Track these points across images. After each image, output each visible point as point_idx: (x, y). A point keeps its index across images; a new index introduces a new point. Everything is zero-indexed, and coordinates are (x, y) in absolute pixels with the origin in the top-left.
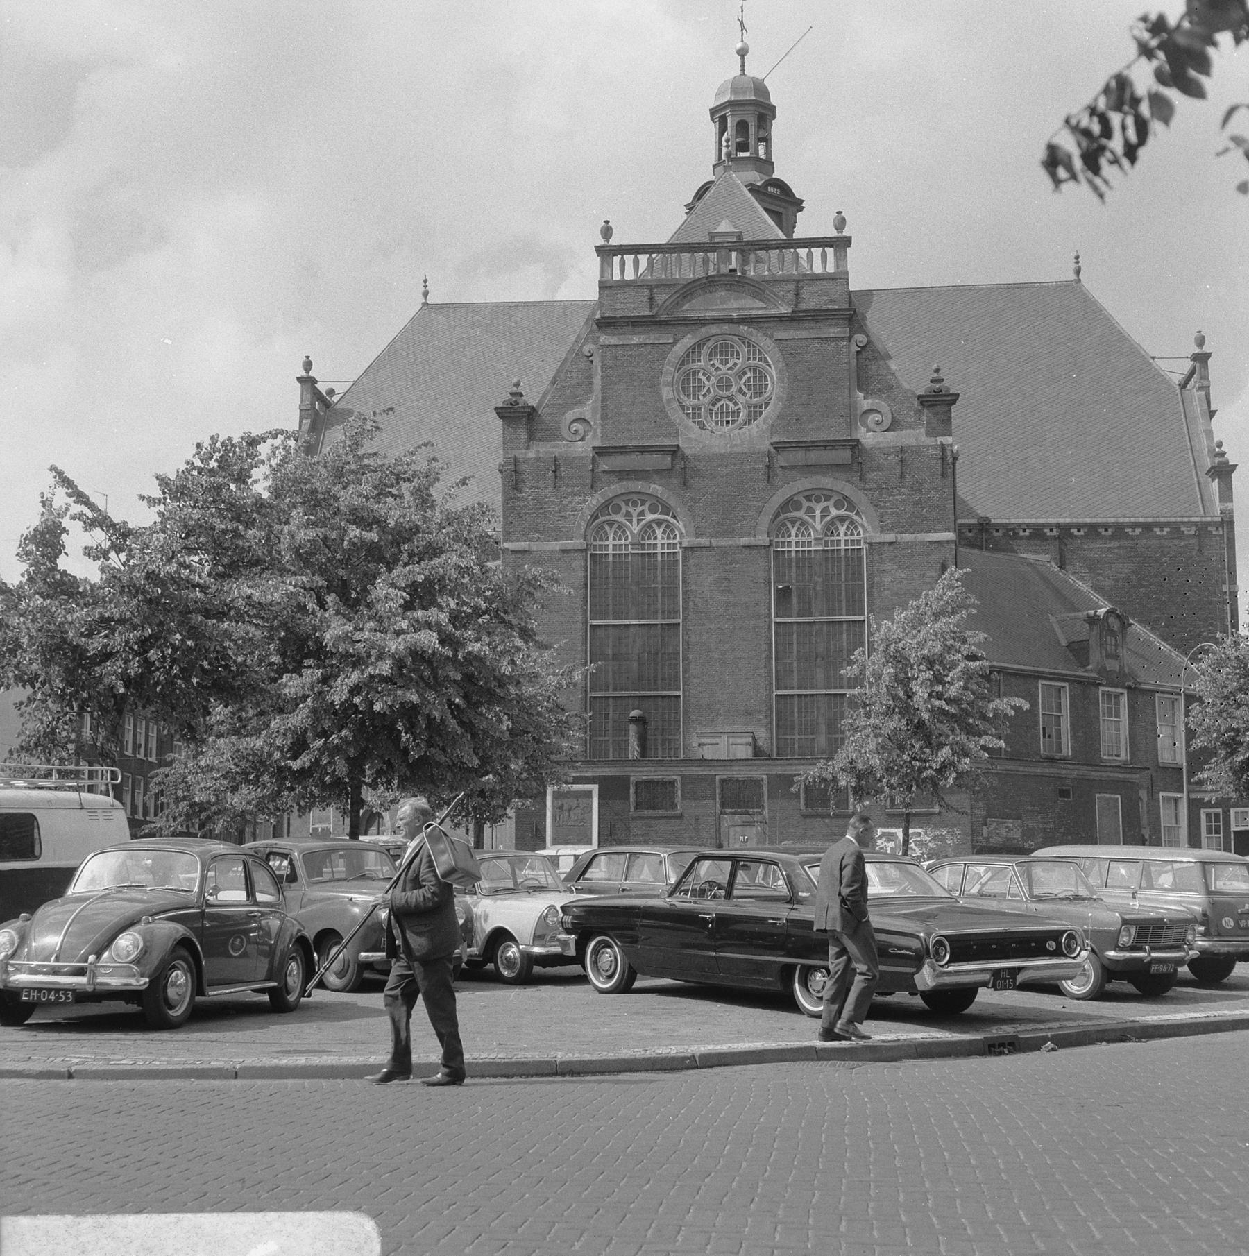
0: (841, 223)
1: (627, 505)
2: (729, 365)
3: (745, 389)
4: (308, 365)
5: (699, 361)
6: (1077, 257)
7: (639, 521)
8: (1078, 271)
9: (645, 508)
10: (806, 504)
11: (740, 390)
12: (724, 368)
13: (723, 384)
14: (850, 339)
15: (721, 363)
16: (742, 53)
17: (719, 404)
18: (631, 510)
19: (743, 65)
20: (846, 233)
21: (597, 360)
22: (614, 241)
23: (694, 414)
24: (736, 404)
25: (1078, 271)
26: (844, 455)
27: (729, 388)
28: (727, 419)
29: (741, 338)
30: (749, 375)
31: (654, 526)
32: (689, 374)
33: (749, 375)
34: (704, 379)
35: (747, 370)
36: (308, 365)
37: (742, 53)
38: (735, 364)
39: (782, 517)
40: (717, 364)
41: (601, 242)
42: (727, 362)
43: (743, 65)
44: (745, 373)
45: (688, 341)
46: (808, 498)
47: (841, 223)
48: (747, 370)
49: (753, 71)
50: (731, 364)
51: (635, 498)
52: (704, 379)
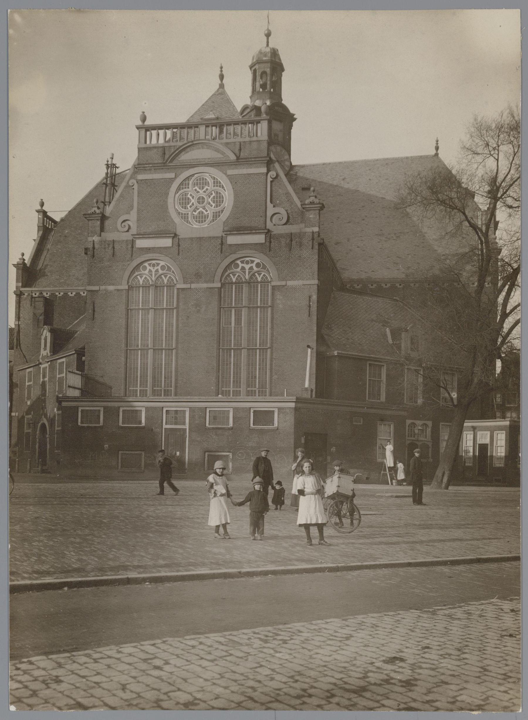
2: (204, 190)
3: (212, 203)
4: (42, 204)
5: (188, 188)
6: (437, 141)
7: (155, 275)
8: (437, 148)
10: (241, 265)
11: (209, 203)
12: (201, 192)
13: (201, 200)
14: (267, 174)
15: (200, 189)
17: (198, 211)
21: (136, 187)
22: (148, 123)
23: (185, 217)
24: (207, 211)
25: (437, 148)
26: (260, 238)
27: (203, 202)
28: (201, 218)
30: (214, 194)
31: (163, 276)
32: (183, 196)
34: (191, 198)
35: (213, 192)
36: (42, 204)
38: (207, 189)
39: (229, 272)
40: (198, 190)
41: (140, 123)
42: (203, 188)
44: (212, 194)
46: (242, 262)
48: (213, 192)
50: (205, 189)
51: (154, 262)
52: (191, 198)
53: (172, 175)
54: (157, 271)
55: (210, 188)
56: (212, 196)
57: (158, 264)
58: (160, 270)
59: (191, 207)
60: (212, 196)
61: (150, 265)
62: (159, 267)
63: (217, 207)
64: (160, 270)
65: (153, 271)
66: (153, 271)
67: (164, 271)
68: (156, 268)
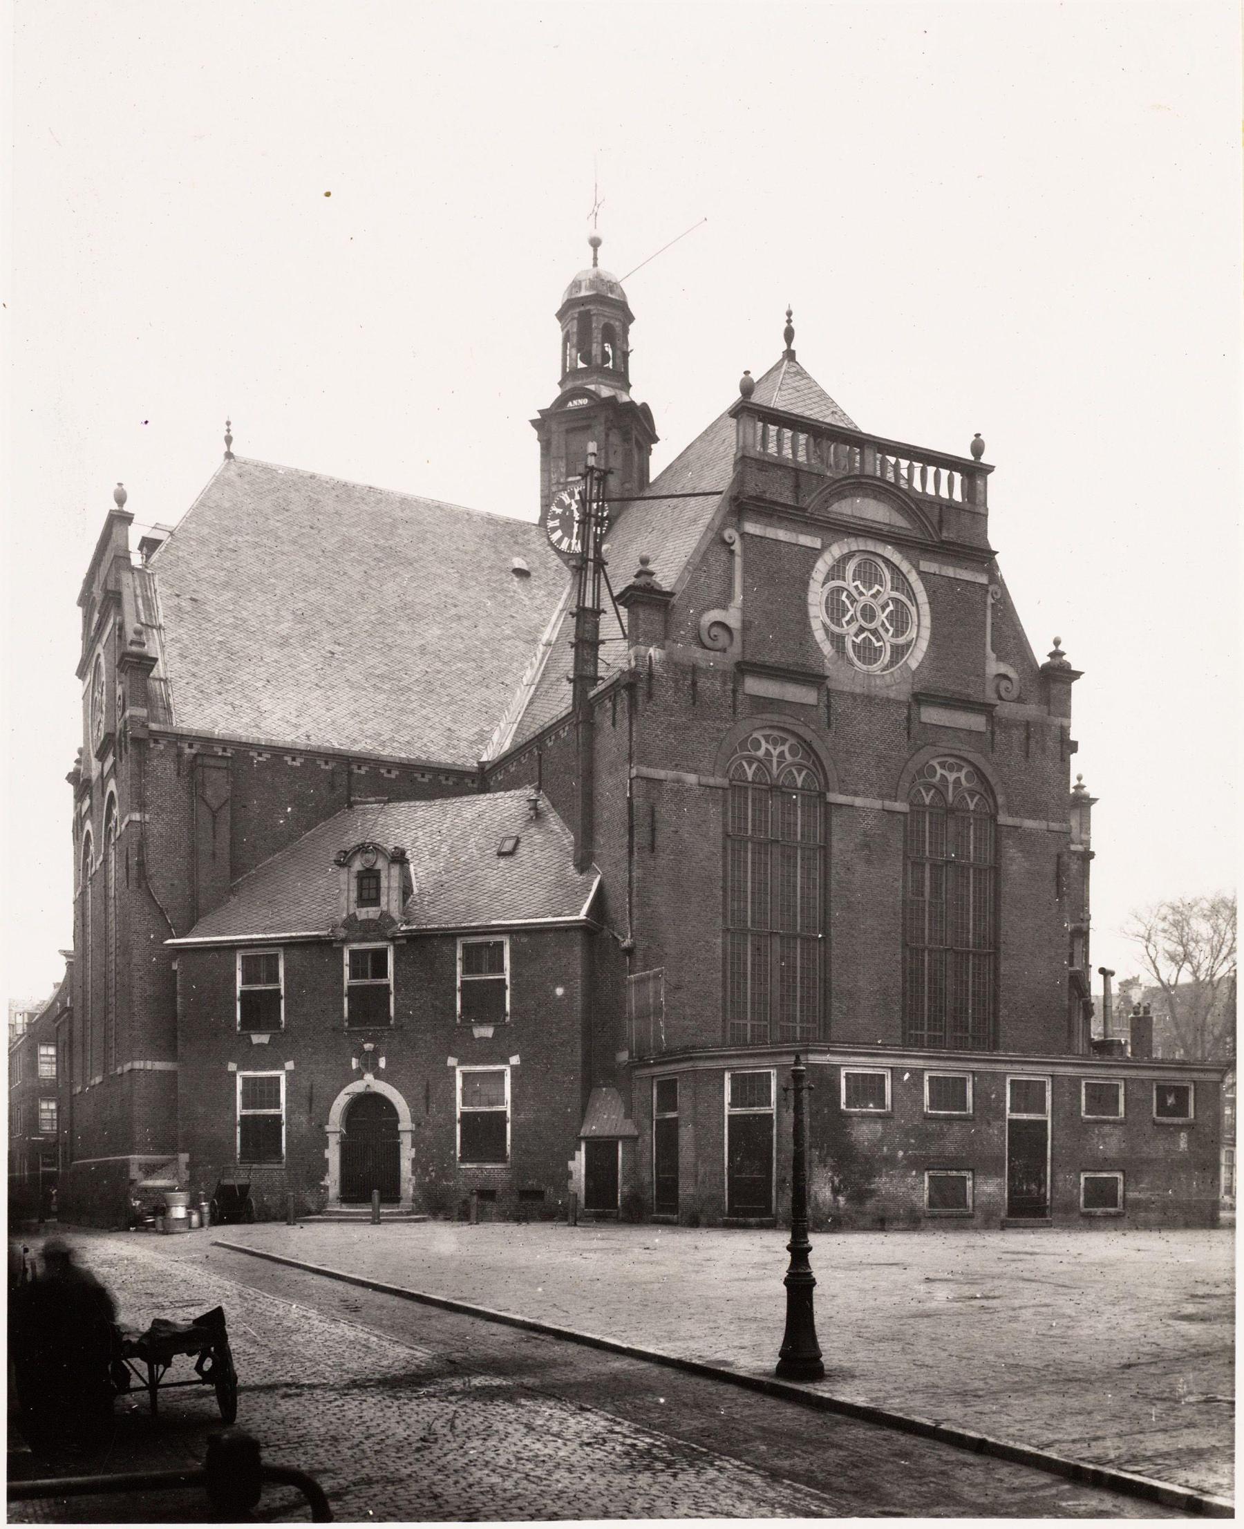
0: (978, 448)
1: (767, 742)
7: (779, 763)
9: (786, 748)
13: (868, 613)
16: (595, 243)
17: (863, 636)
18: (770, 748)
19: (595, 258)
20: (985, 459)
29: (887, 561)
33: (891, 607)
37: (595, 243)
42: (870, 588)
43: (595, 258)
44: (887, 605)
45: (836, 551)
47: (978, 448)
49: (611, 267)
53: (817, 543)
54: (782, 754)
55: (888, 592)
56: (888, 610)
57: (784, 741)
58: (787, 755)
59: (848, 623)
60: (888, 610)
61: (767, 738)
62: (786, 748)
63: (897, 637)
64: (787, 755)
65: (775, 753)
66: (775, 753)
67: (797, 759)
68: (779, 749)
